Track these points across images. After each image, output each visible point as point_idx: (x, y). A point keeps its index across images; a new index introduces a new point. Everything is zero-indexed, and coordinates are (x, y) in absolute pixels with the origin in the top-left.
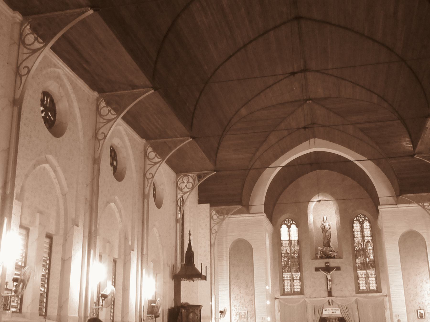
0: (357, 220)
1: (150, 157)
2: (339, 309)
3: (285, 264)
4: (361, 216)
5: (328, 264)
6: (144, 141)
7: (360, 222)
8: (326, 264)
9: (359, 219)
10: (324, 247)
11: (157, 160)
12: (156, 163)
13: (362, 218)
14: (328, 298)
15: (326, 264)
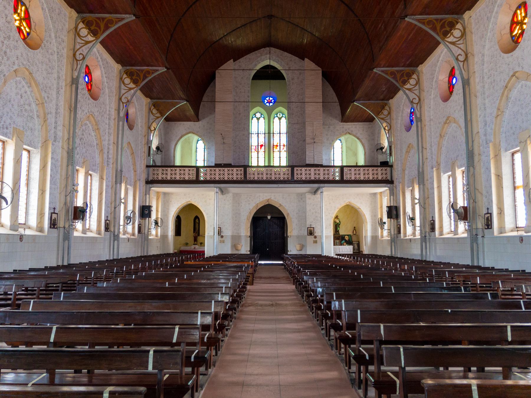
1: (81, 34)
6: (74, 14)
11: (90, 38)
12: (87, 43)
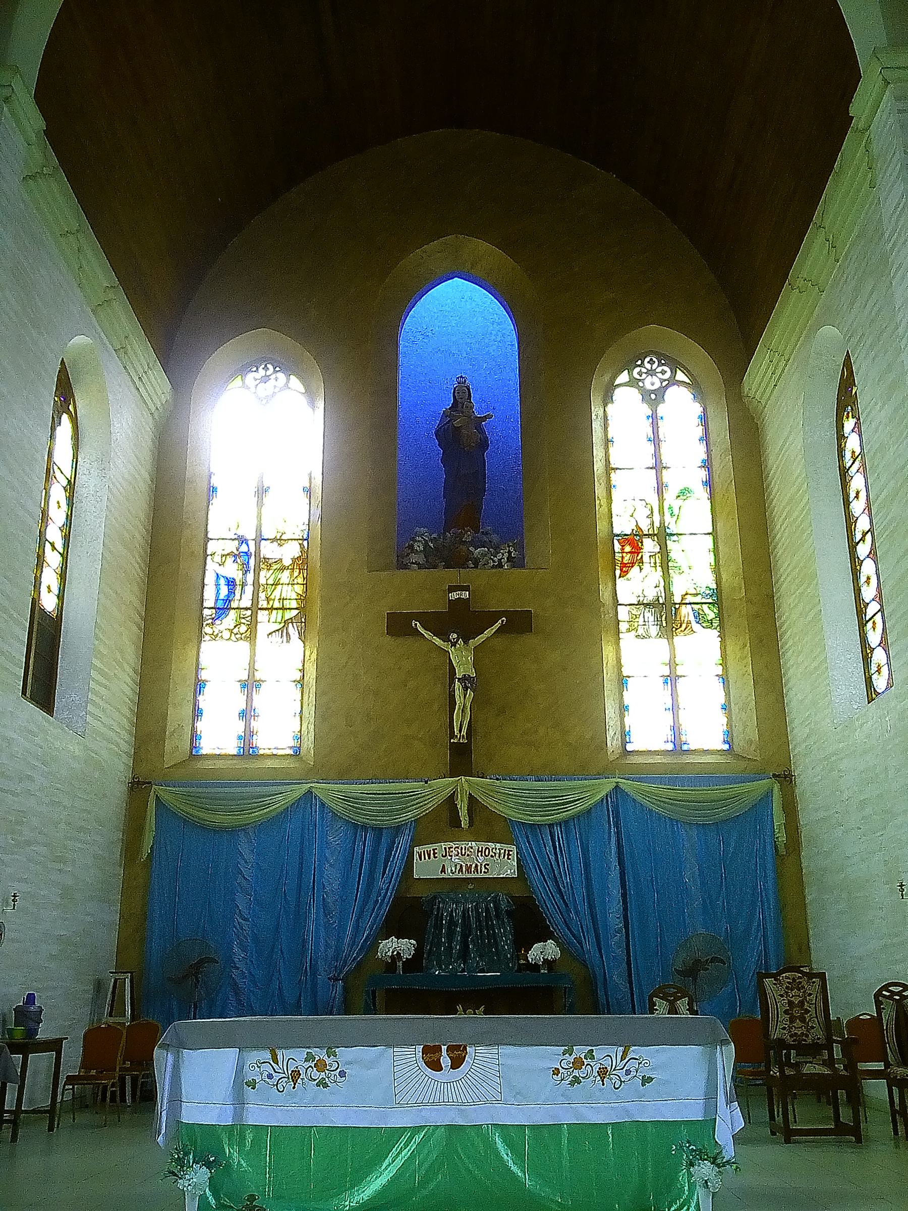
0: (633, 383)
2: (507, 847)
3: (222, 597)
4: (651, 362)
5: (465, 595)
7: (646, 395)
8: (454, 596)
9: (642, 381)
10: (447, 529)
13: (660, 375)
14: (444, 785)
15: (454, 596)
